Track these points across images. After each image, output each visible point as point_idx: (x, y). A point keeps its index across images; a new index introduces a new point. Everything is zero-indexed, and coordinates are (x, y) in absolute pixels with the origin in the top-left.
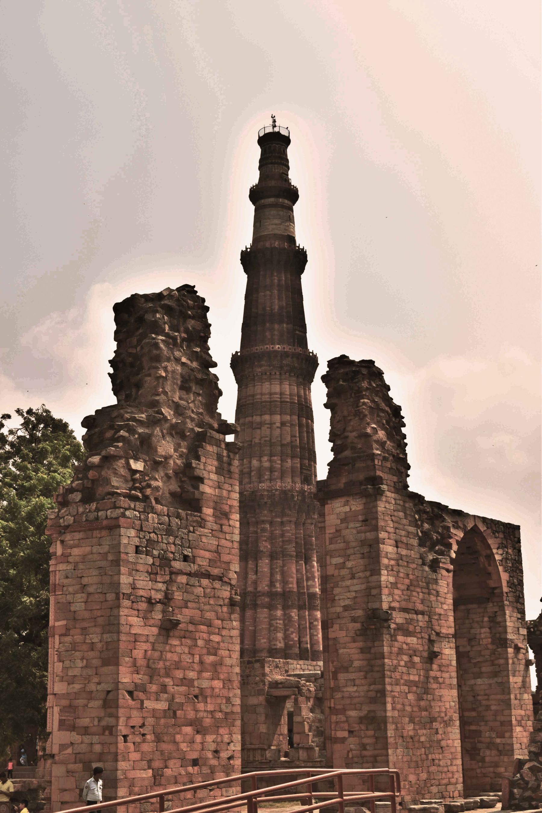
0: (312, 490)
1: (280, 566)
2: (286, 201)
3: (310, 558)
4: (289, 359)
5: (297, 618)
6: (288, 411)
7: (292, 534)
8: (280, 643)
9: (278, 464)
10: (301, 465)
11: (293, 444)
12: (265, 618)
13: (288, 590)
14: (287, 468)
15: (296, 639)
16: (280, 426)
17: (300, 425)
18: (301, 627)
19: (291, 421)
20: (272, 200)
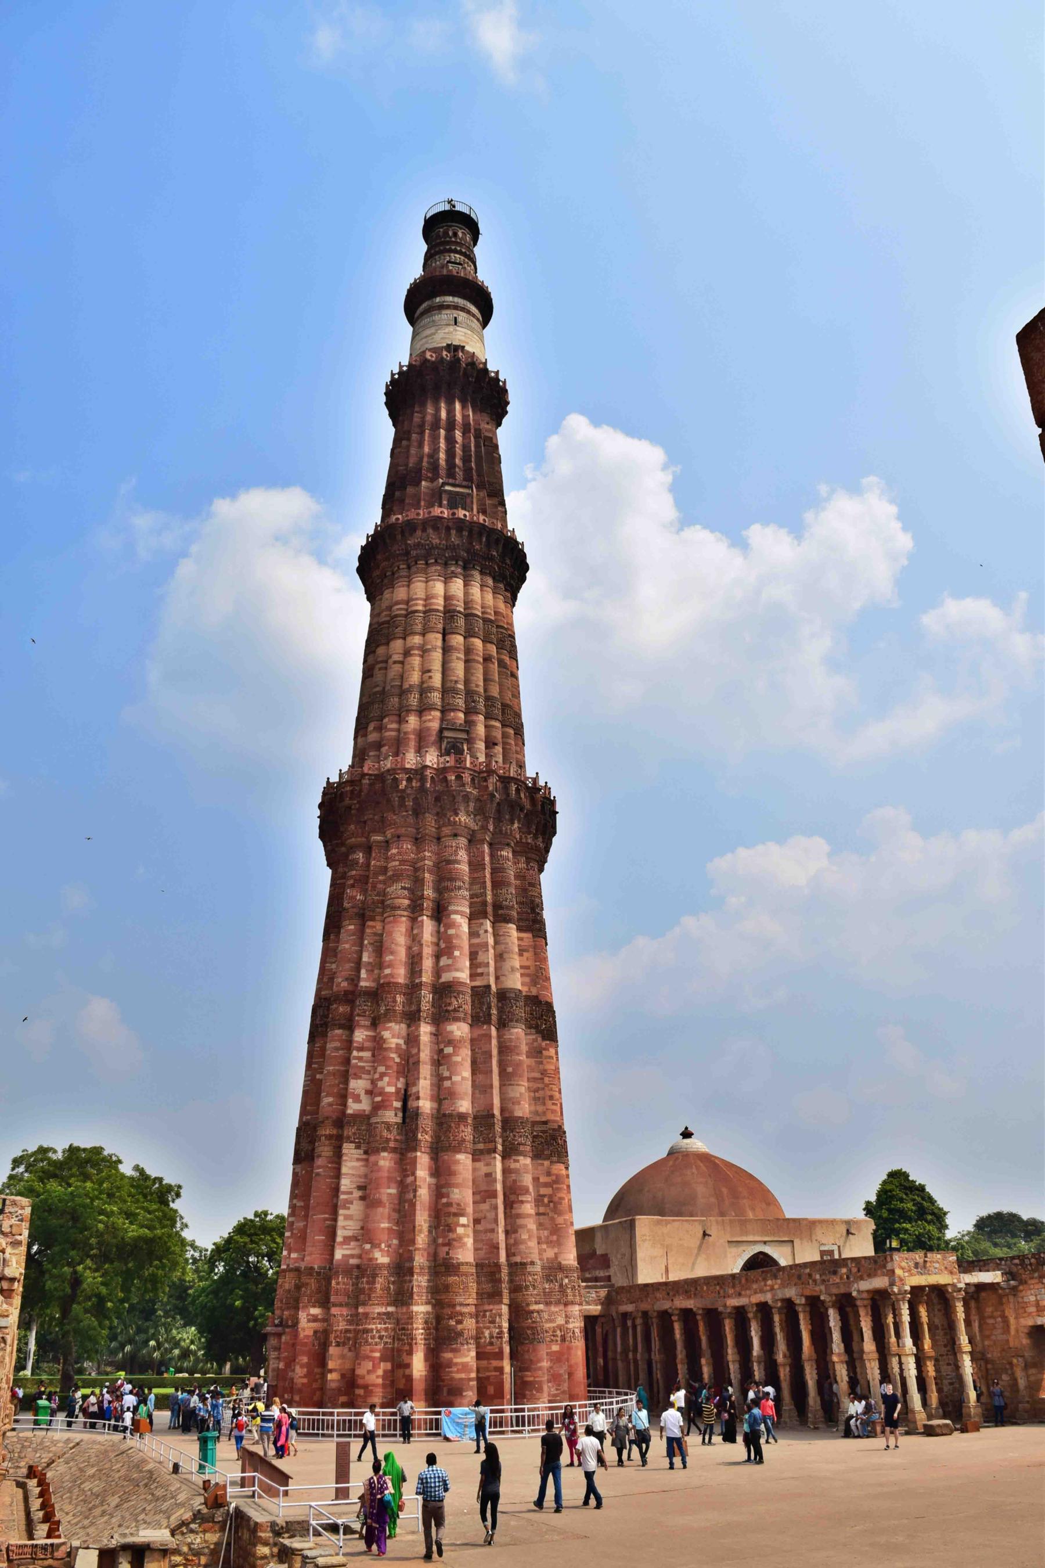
0: (448, 765)
1: (375, 934)
2: (449, 299)
3: (445, 909)
4: (419, 533)
5: (401, 1042)
6: (419, 628)
7: (403, 862)
8: (360, 1102)
9: (392, 730)
10: (442, 720)
11: (425, 685)
12: (337, 1049)
13: (382, 981)
14: (406, 733)
15: (391, 1089)
16: (401, 659)
17: (446, 649)
18: (411, 1061)
19: (424, 645)
20: (425, 305)
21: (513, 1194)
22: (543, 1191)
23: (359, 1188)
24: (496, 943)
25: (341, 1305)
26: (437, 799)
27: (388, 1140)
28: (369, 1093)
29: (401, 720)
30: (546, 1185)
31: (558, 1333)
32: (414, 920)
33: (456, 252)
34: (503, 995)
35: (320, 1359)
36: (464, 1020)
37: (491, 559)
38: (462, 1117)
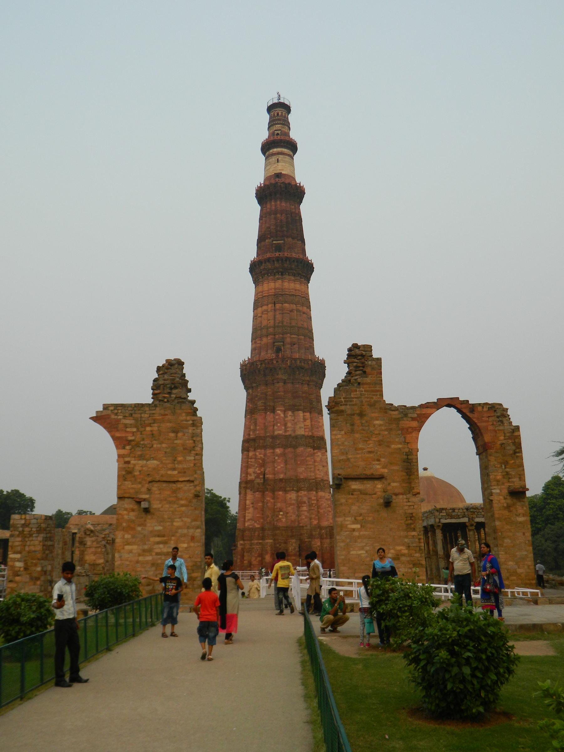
2: (275, 150)
4: (263, 264)
5: (262, 456)
17: (275, 310)
21: (299, 504)
22: (313, 502)
23: (252, 503)
24: (295, 419)
25: (247, 540)
26: (271, 370)
27: (258, 488)
28: (254, 472)
29: (261, 340)
30: (314, 500)
31: (318, 548)
32: (266, 413)
33: (278, 124)
34: (296, 437)
35: (243, 556)
36: (281, 447)
37: (291, 269)
38: (281, 480)
